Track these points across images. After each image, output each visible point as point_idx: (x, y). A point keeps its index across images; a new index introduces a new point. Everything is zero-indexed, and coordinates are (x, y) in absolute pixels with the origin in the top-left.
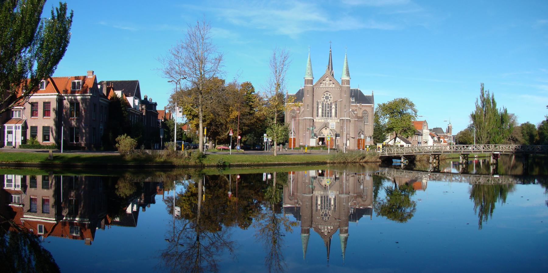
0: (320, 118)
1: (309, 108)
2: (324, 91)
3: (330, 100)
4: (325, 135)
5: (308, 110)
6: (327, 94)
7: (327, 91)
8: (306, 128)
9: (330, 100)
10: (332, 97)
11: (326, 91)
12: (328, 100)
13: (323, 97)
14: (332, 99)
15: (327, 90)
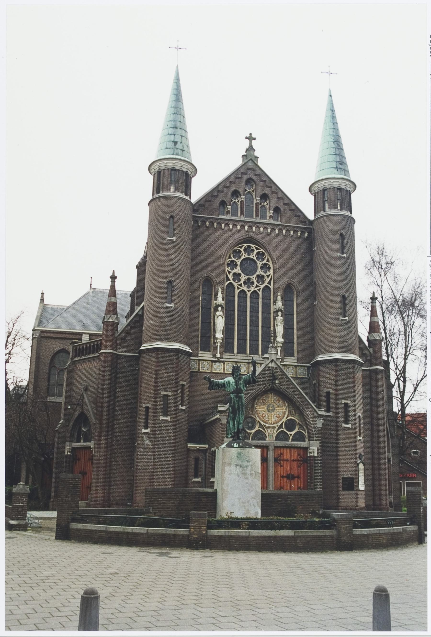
0: (218, 355)
1: (176, 299)
2: (237, 237)
3: (260, 278)
4: (267, 432)
5: (172, 305)
6: (248, 250)
7: (249, 240)
8: (156, 395)
9: (260, 278)
10: (271, 264)
11: (243, 235)
12: (254, 278)
13: (232, 264)
14: (271, 272)
15: (250, 234)
